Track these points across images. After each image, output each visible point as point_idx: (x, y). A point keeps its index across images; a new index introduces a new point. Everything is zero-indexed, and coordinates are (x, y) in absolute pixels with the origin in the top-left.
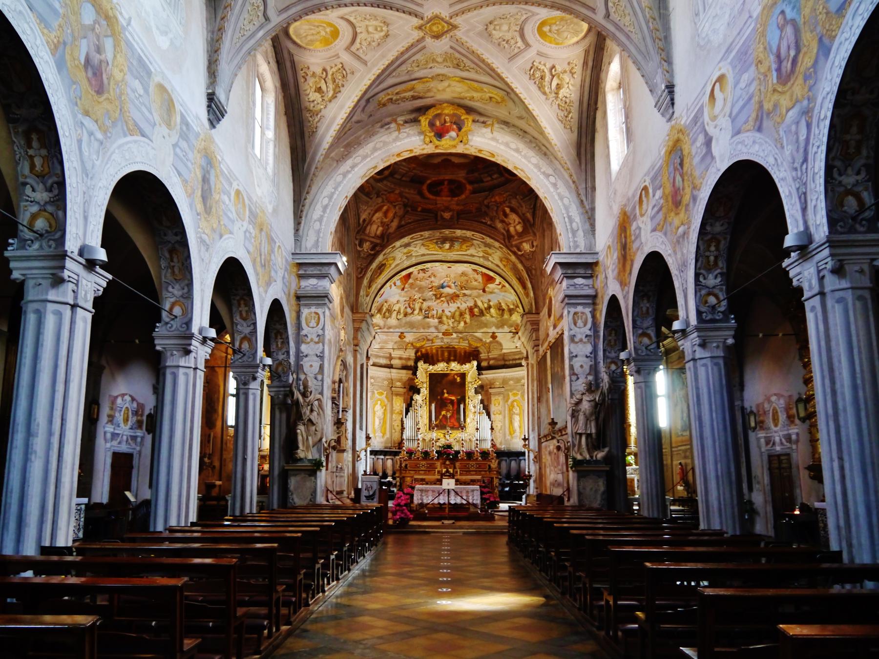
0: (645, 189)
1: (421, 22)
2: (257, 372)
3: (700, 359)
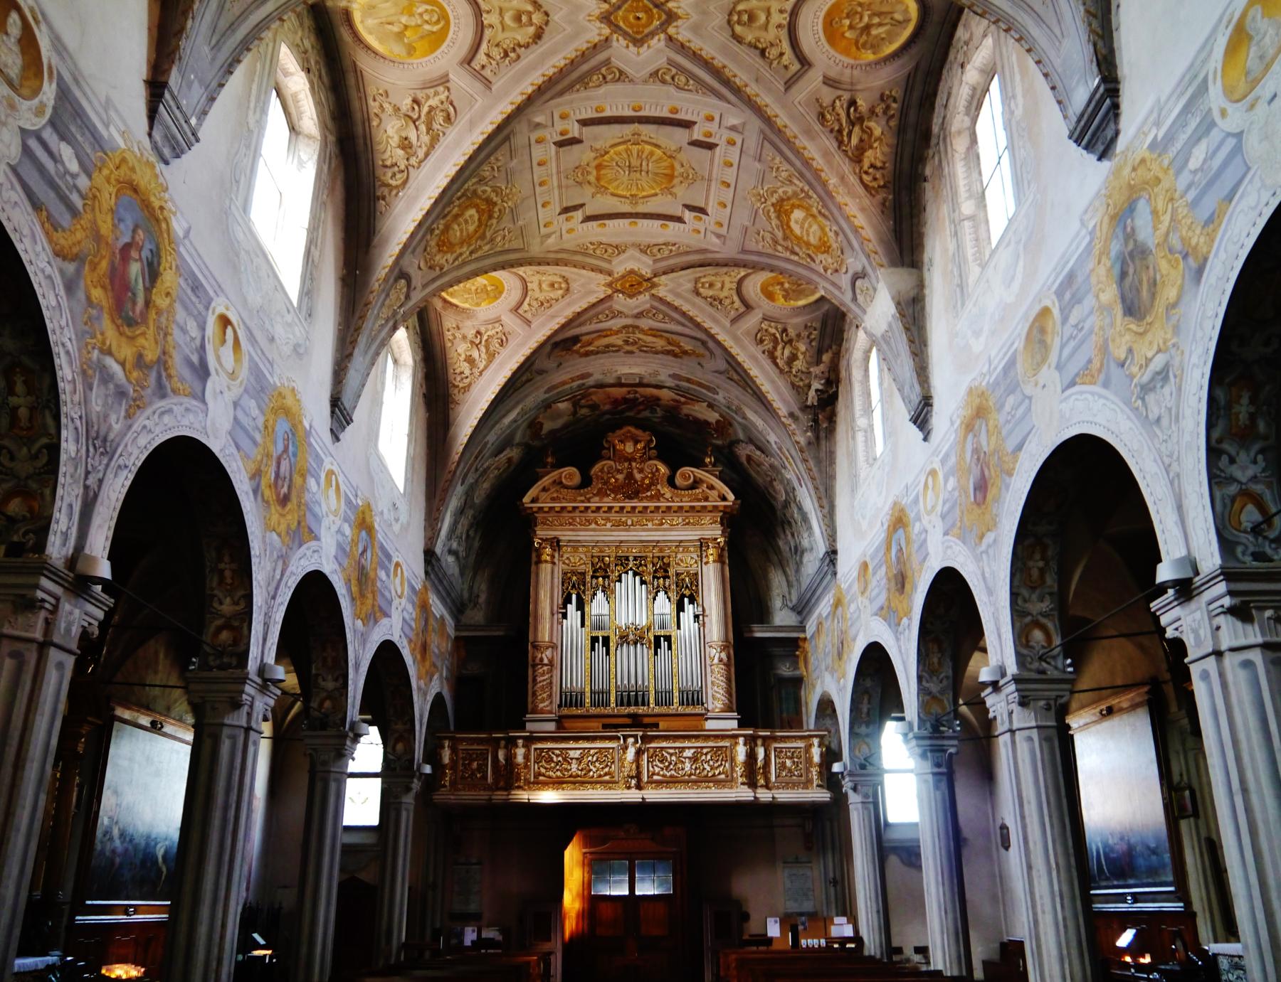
0: (933, 473)
1: (609, 279)
3: (1019, 729)
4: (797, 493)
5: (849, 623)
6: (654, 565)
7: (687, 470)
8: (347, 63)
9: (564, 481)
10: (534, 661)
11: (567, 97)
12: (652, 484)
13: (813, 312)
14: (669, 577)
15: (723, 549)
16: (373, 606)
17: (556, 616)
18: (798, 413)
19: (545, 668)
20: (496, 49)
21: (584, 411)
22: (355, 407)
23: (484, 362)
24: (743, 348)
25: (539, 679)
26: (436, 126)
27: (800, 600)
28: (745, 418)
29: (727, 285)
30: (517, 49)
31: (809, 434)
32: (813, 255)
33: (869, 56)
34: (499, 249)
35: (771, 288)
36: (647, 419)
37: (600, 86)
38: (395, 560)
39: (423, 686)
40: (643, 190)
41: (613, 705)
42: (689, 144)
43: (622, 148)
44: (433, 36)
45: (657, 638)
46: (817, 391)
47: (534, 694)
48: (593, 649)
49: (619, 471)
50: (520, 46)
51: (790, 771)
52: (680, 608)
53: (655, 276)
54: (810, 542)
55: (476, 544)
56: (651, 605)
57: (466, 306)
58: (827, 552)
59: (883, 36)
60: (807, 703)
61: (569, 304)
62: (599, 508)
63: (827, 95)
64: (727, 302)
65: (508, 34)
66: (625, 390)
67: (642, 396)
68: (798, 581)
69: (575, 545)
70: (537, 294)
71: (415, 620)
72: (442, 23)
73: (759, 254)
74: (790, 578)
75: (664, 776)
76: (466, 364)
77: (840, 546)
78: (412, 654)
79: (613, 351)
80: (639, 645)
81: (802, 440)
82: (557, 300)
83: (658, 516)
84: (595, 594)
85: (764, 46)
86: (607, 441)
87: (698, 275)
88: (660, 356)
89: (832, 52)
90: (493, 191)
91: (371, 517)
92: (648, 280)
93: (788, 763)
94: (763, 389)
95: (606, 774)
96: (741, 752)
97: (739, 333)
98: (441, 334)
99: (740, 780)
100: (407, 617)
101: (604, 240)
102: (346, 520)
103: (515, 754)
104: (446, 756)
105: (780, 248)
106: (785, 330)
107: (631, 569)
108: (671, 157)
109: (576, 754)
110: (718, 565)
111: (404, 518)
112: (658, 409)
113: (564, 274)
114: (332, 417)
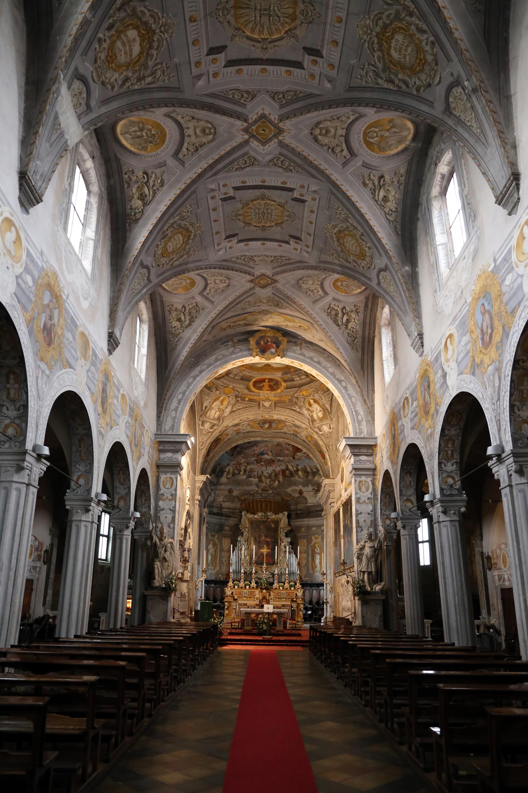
11: (308, 90)
42: (226, 47)
43: (275, 36)
108: (238, 29)
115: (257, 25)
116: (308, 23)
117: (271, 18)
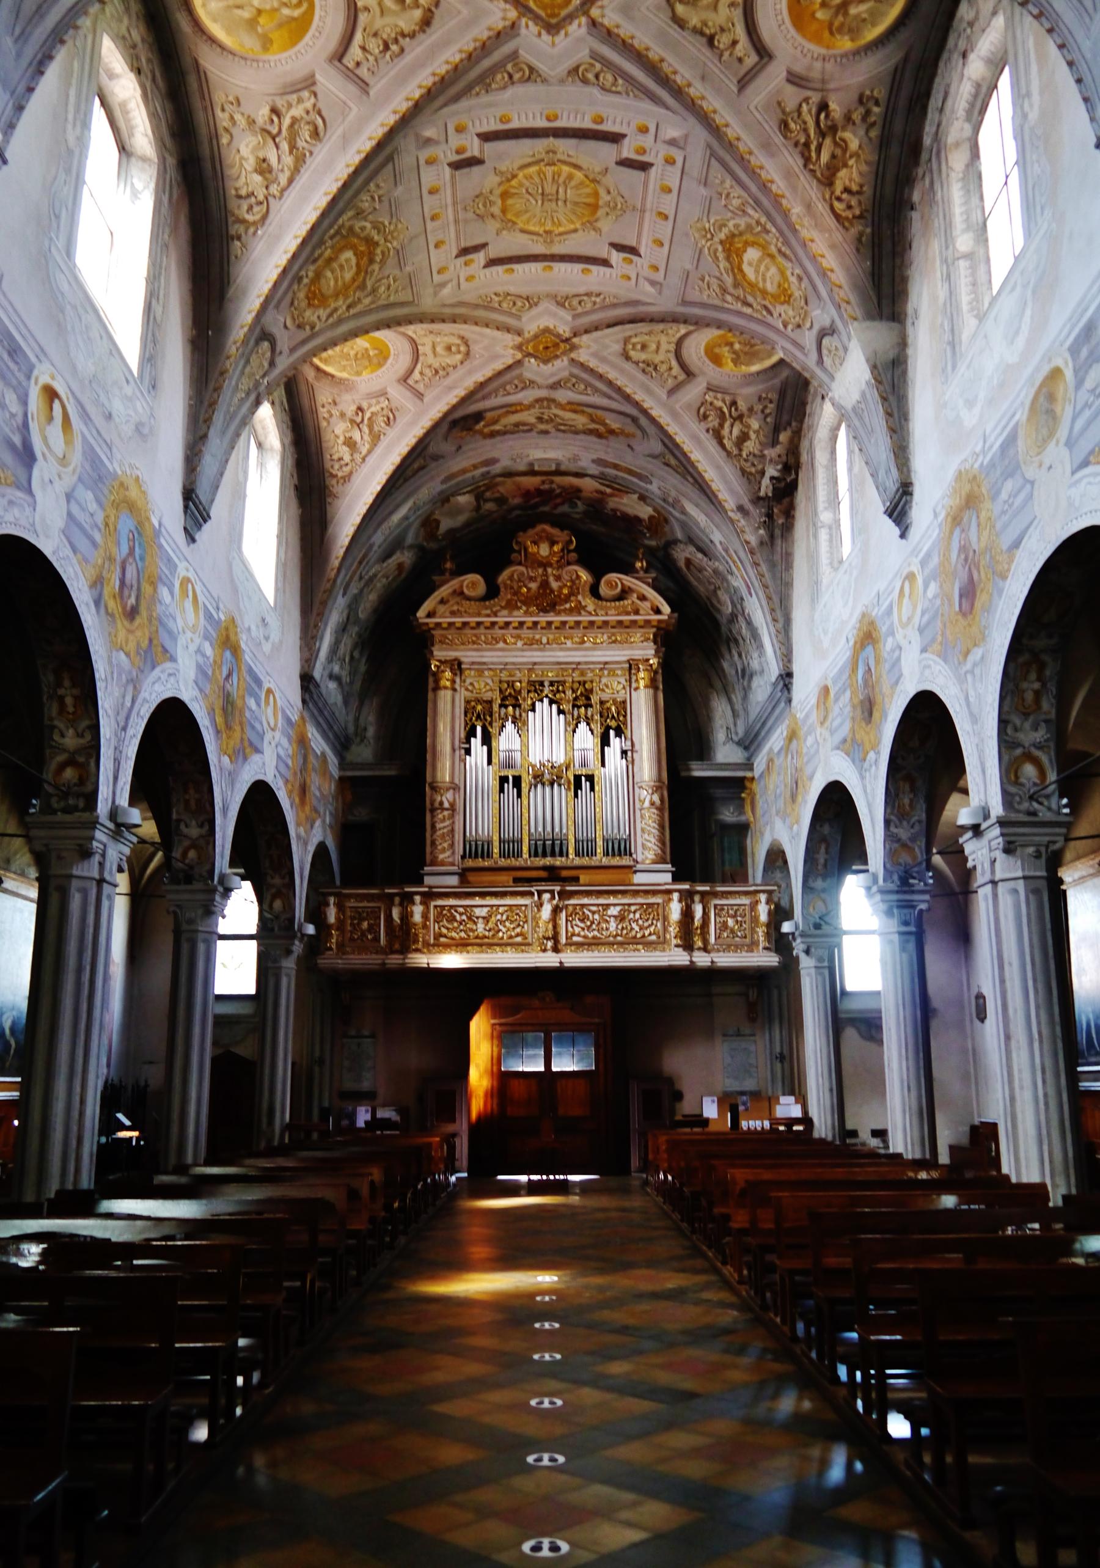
1: (518, 340)
2: (293, 944)
3: (1002, 880)
4: (746, 604)
5: (805, 760)
6: (574, 691)
7: (613, 576)
8: (187, 62)
9: (465, 591)
10: (432, 804)
11: (464, 104)
12: (571, 594)
13: (772, 378)
14: (591, 706)
15: (656, 672)
16: (242, 739)
17: (457, 753)
18: (749, 506)
19: (446, 813)
20: (373, 40)
21: (489, 506)
22: (212, 501)
23: (367, 446)
24: (683, 426)
25: (438, 826)
26: (301, 144)
27: (747, 733)
28: (684, 512)
29: (664, 346)
30: (400, 39)
31: (762, 532)
32: (770, 307)
33: (846, 44)
34: (381, 302)
35: (717, 350)
36: (564, 515)
37: (505, 87)
38: (266, 685)
39: (303, 833)
40: (560, 225)
41: (525, 855)
43: (533, 169)
44: (294, 25)
45: (578, 778)
46: (772, 478)
47: (433, 843)
48: (502, 790)
49: (532, 579)
50: (404, 35)
51: (732, 931)
52: (605, 742)
53: (575, 335)
54: (760, 663)
55: (363, 668)
56: (570, 739)
57: (344, 375)
58: (781, 676)
59: (864, 16)
60: (753, 854)
61: (470, 372)
62: (507, 624)
63: (792, 96)
64: (663, 368)
65: (388, 20)
66: (537, 480)
67: (559, 486)
68: (746, 710)
69: (480, 668)
70: (431, 359)
71: (292, 758)
72: (305, 5)
73: (703, 305)
74: (736, 707)
75: (585, 937)
76: (346, 449)
77: (796, 668)
78: (290, 797)
79: (524, 431)
80: (556, 785)
81: (753, 540)
82: (455, 367)
83: (577, 634)
84: (503, 726)
85: (713, 31)
86: (518, 543)
87: (628, 334)
88: (582, 437)
89: (800, 39)
90: (374, 228)
91: (236, 634)
92: (567, 340)
93: (731, 922)
94: (707, 476)
95: (517, 935)
96: (675, 910)
97: (677, 407)
98: (314, 411)
99: (674, 942)
100: (282, 753)
101: (512, 290)
102: (206, 637)
103: (412, 912)
104: (332, 914)
105: (729, 298)
106: (734, 403)
107: (547, 696)
108: (594, 181)
109: (483, 912)
110: (651, 691)
111: (275, 636)
112: (579, 503)
113: (462, 333)
114: (185, 512)
115: (564, 182)
116: (481, 194)
117: (540, 191)
